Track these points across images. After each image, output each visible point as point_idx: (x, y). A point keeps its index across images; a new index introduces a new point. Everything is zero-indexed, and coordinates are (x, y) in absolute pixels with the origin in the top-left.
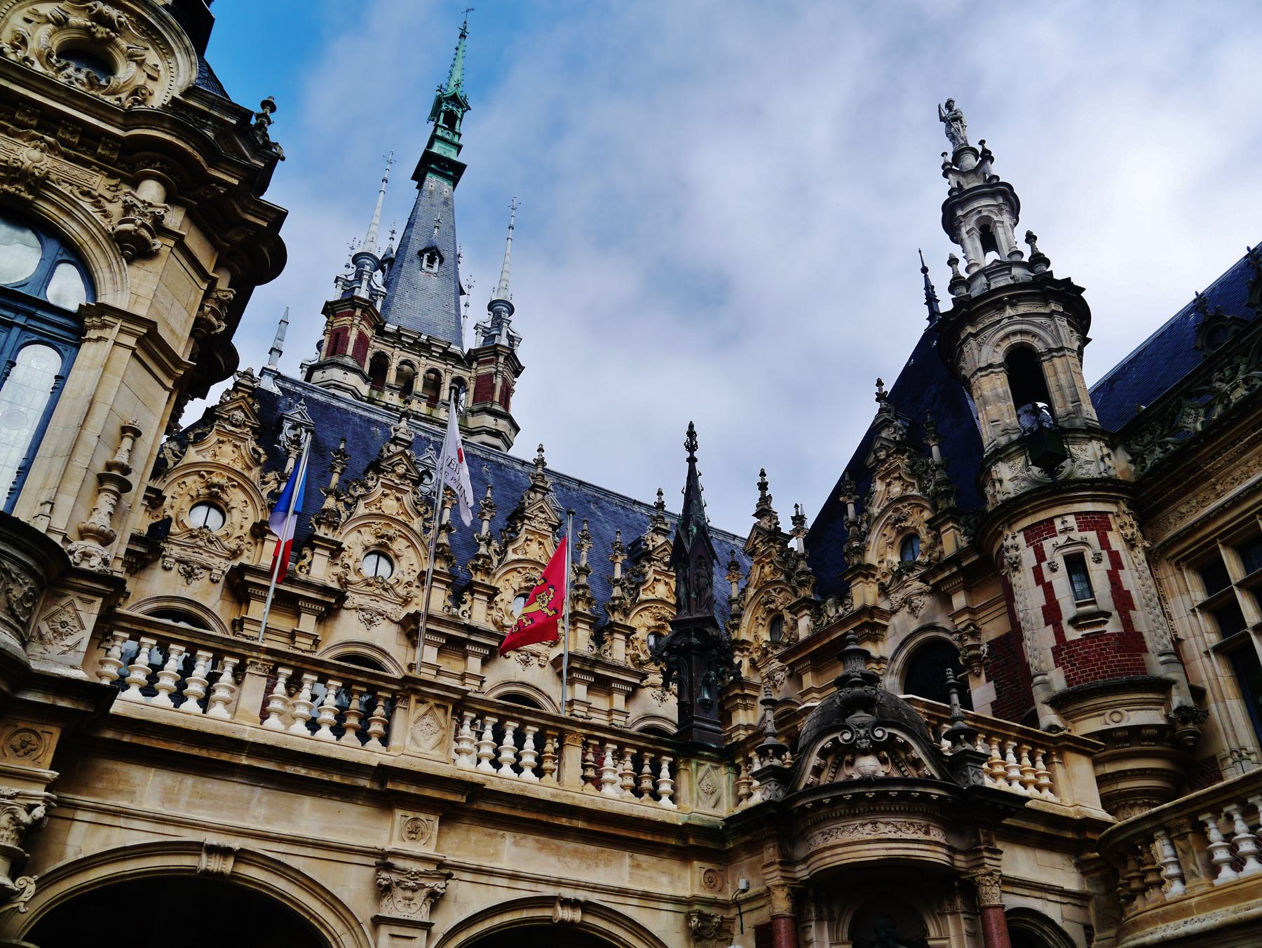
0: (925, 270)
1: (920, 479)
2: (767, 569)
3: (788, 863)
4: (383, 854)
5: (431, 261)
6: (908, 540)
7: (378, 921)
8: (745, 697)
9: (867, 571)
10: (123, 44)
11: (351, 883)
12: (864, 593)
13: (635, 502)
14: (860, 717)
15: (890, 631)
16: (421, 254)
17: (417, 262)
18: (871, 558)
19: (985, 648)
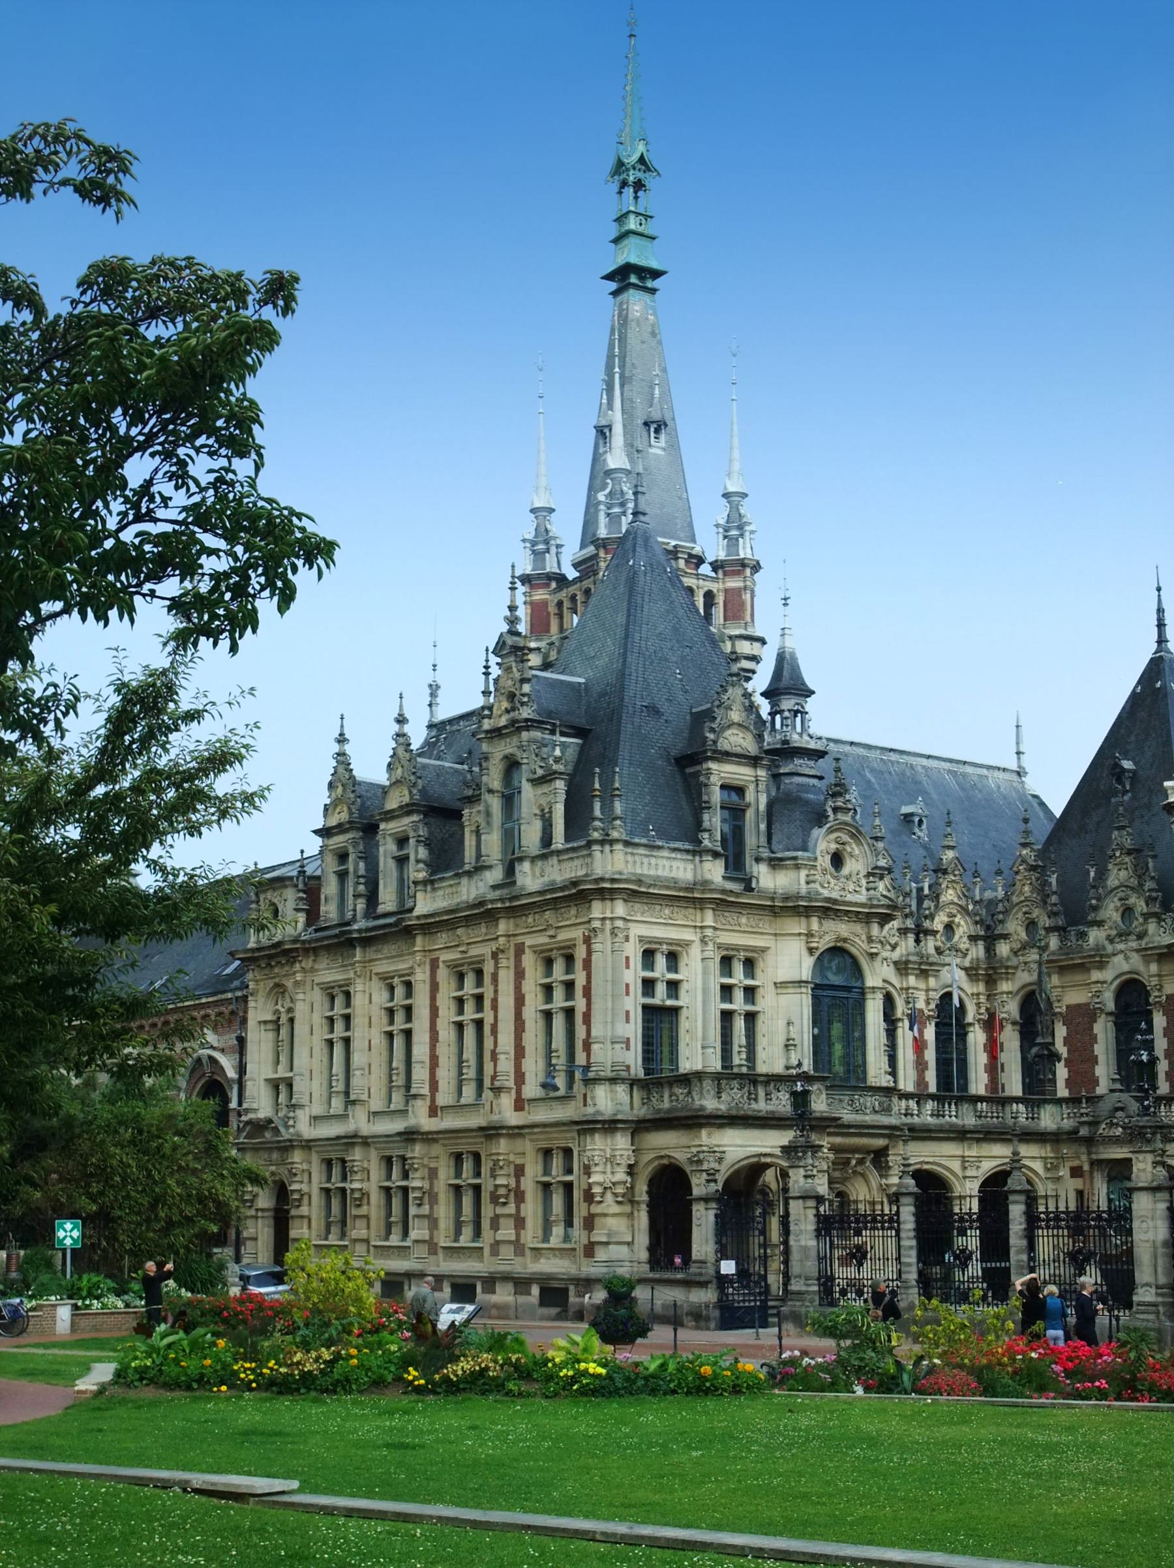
0: (1159, 589)
1: (1139, 877)
2: (1026, 888)
3: (1089, 1153)
4: (963, 1157)
5: (657, 431)
6: (1127, 912)
7: (965, 1177)
8: (1007, 973)
9: (1099, 924)
10: (849, 849)
11: (956, 1165)
12: (1095, 936)
13: (891, 750)
14: (1119, 1114)
15: (1110, 965)
16: (646, 424)
17: (645, 434)
18: (1102, 915)
19: (1164, 998)
